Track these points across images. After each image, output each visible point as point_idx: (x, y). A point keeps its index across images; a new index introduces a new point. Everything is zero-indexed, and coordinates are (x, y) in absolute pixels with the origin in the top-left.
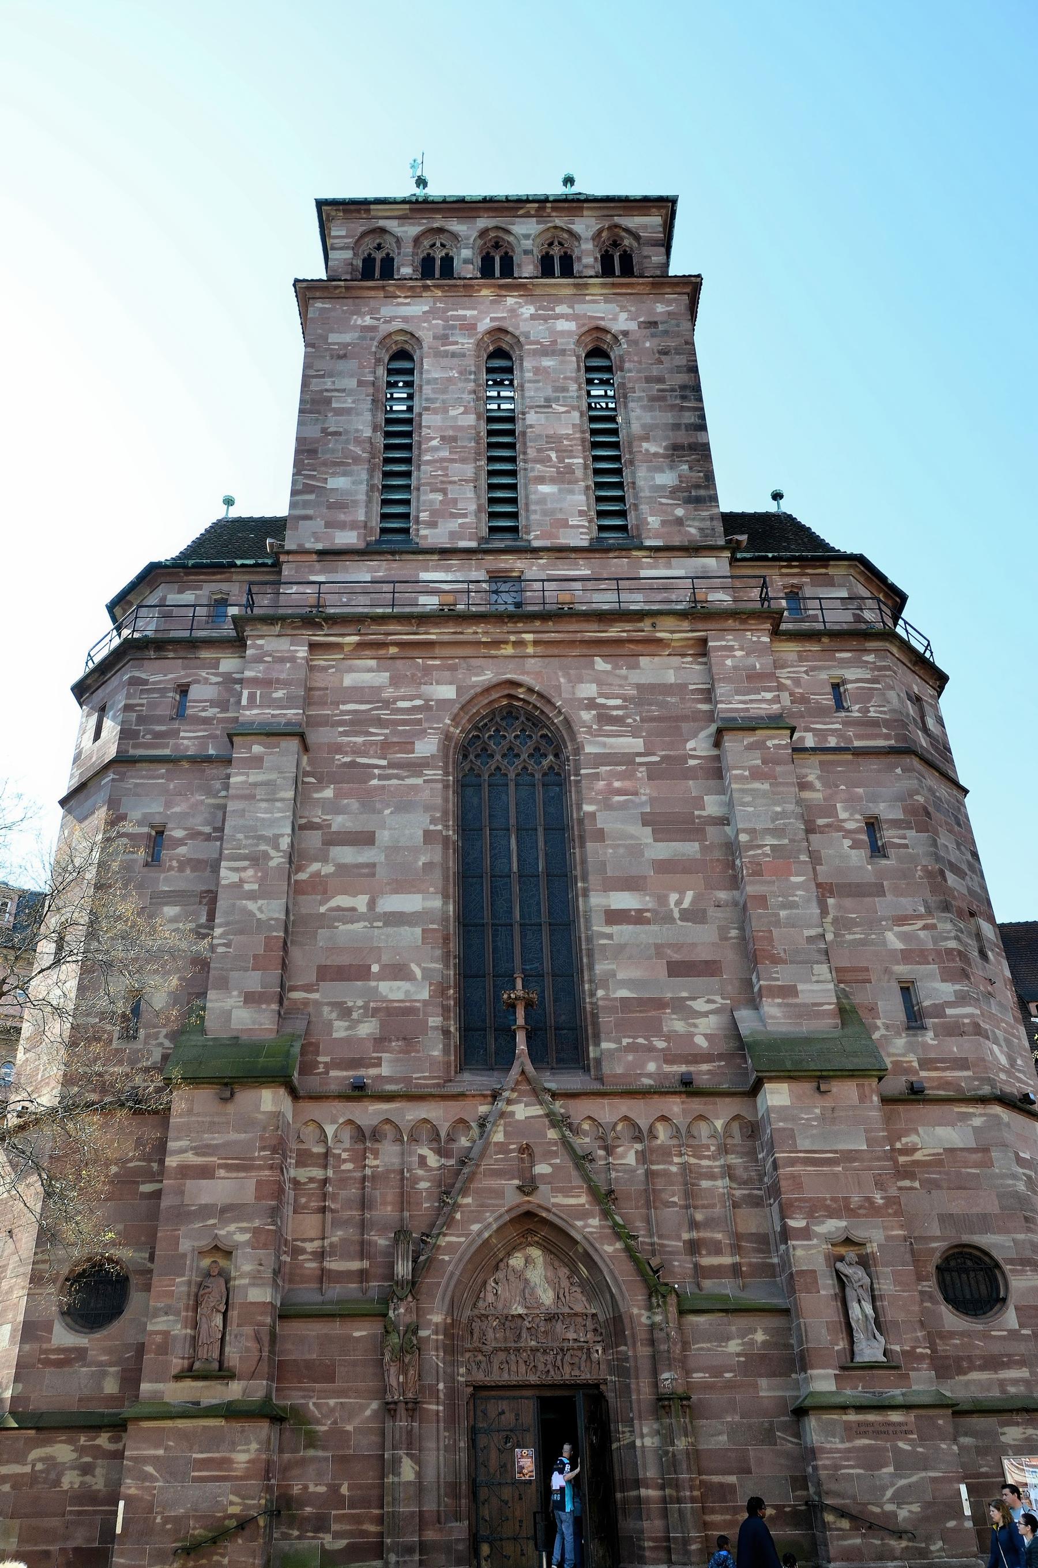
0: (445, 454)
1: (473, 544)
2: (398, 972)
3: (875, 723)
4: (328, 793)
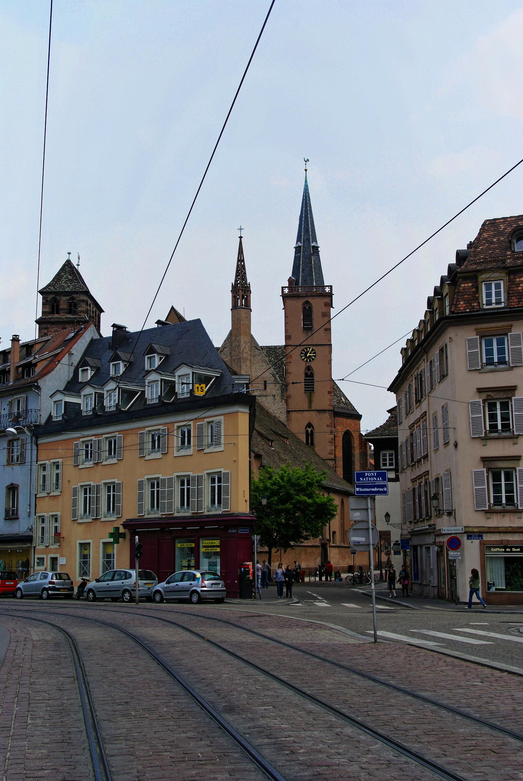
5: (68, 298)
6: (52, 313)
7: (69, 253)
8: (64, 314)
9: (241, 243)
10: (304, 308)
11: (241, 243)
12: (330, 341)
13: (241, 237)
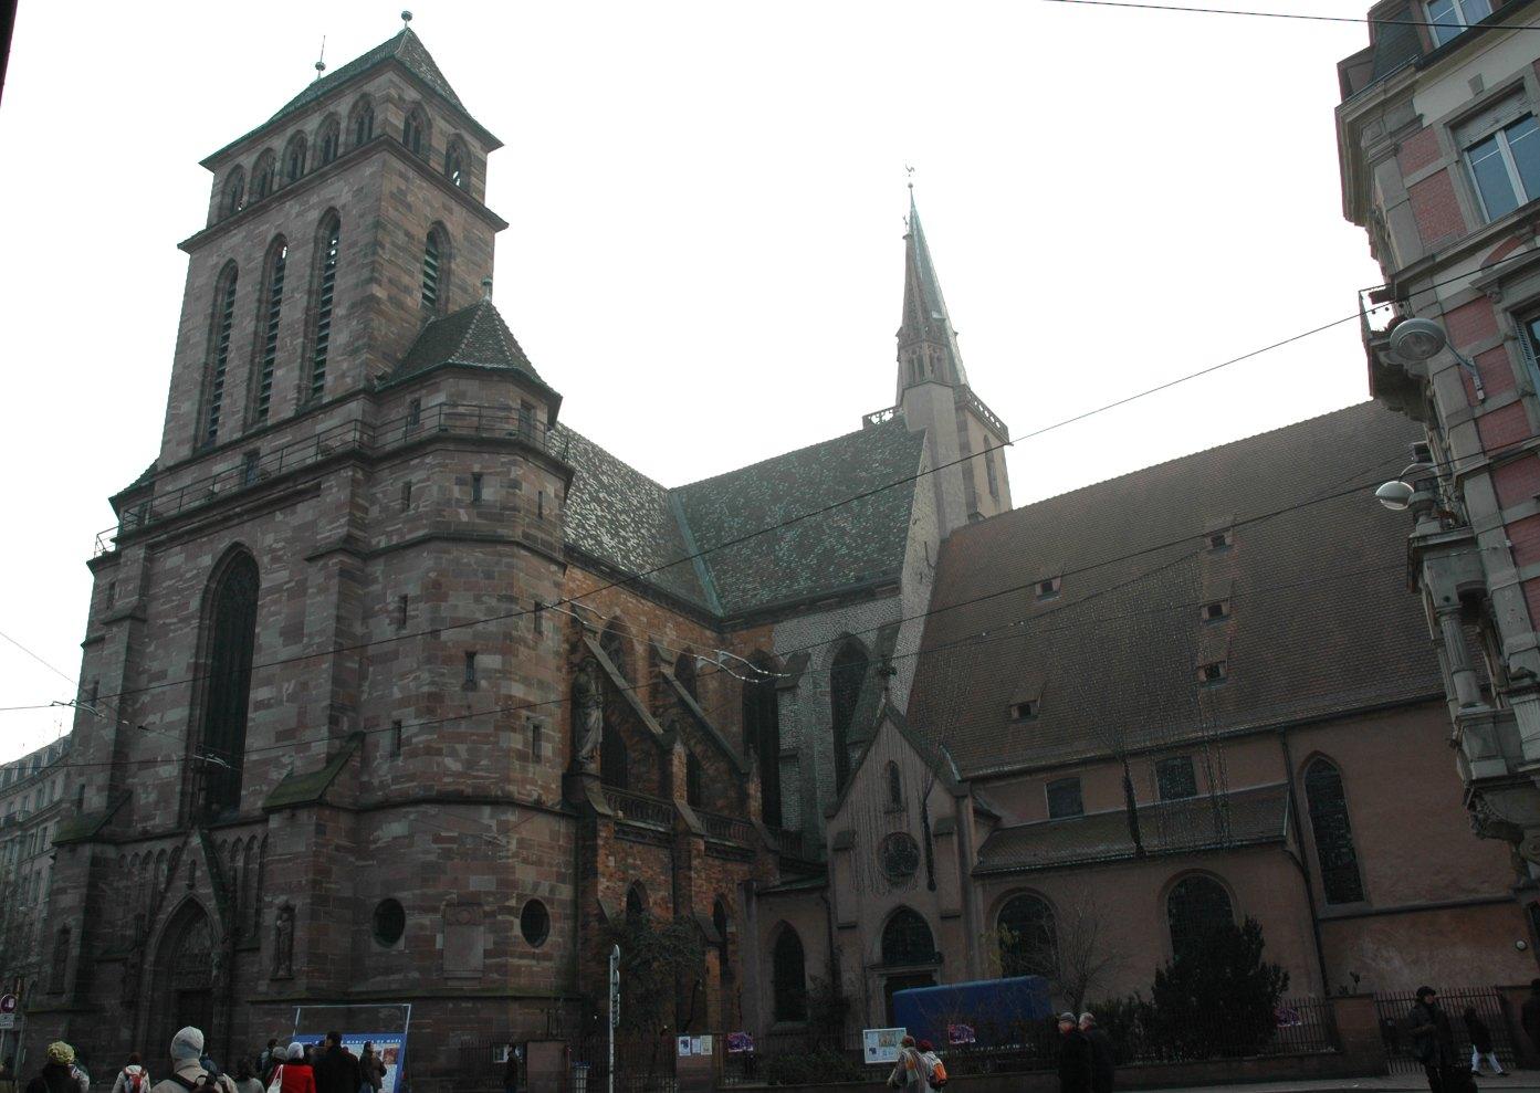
0: (236, 362)
1: (237, 435)
2: (167, 761)
3: (420, 517)
4: (152, 648)
5: (452, 131)
7: (407, 16)
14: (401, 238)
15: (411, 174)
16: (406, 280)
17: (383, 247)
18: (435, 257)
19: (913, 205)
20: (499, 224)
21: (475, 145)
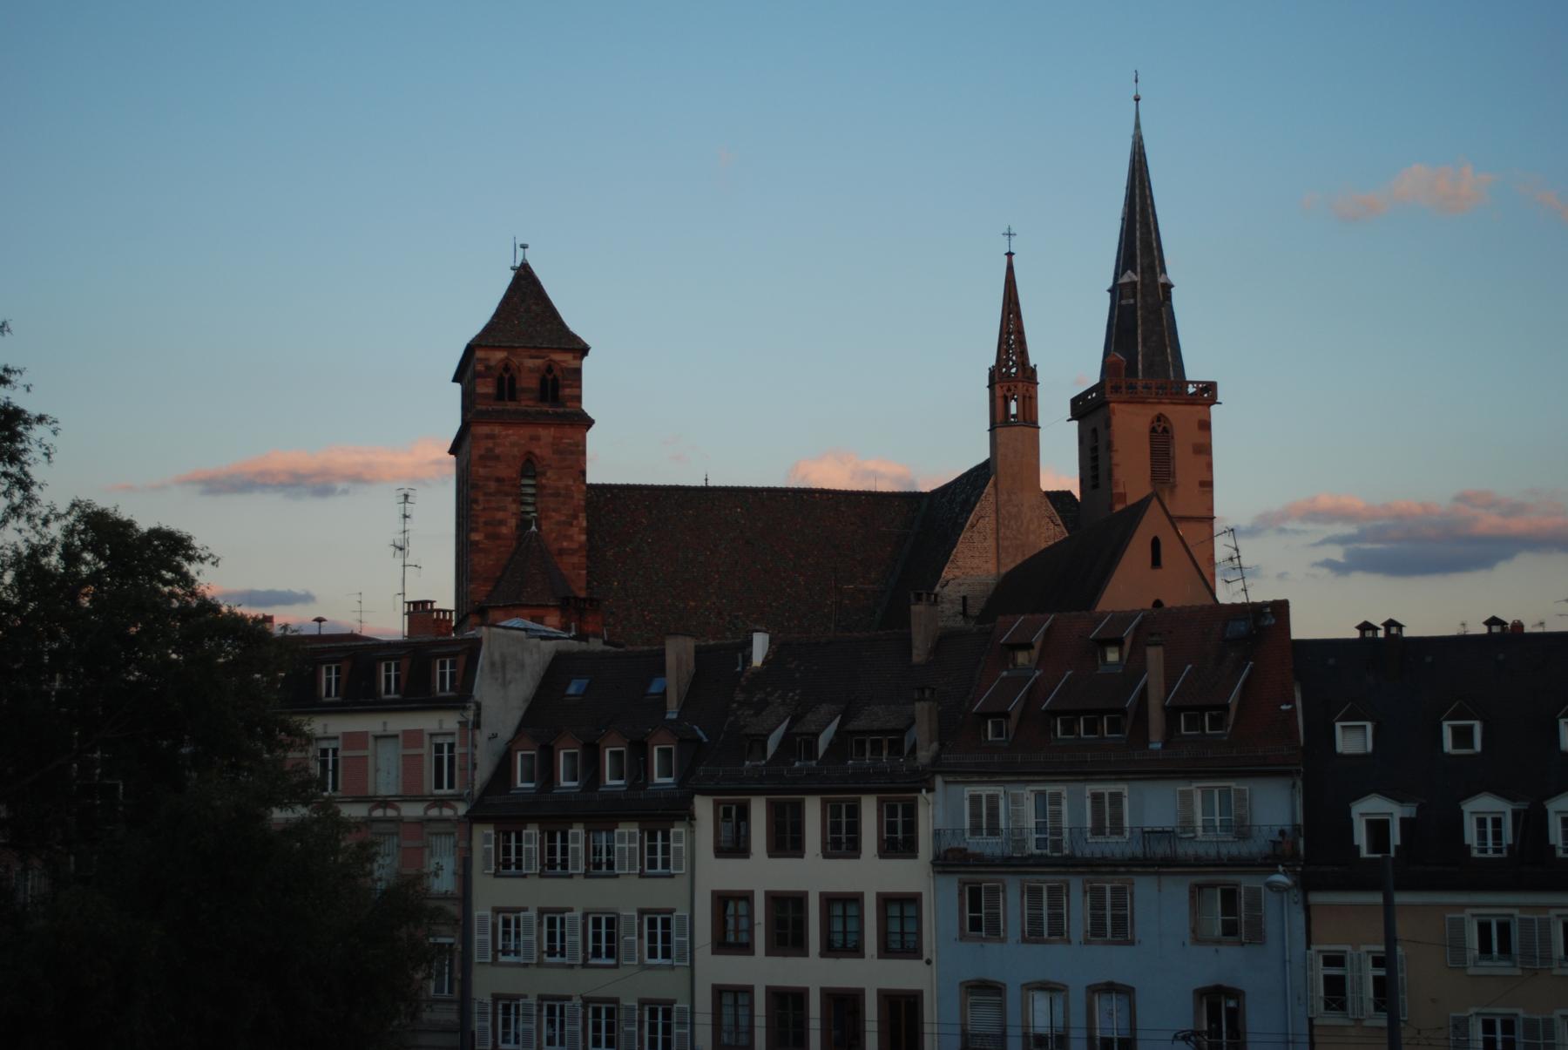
5: (539, 362)
6: (500, 397)
7: (524, 247)
8: (531, 403)
9: (1010, 268)
10: (1153, 430)
11: (1010, 268)
12: (1211, 509)
13: (1010, 254)
14: (493, 486)
15: (497, 429)
16: (500, 515)
17: (476, 501)
18: (533, 477)
19: (1138, 126)
20: (589, 423)
21: (567, 359)
